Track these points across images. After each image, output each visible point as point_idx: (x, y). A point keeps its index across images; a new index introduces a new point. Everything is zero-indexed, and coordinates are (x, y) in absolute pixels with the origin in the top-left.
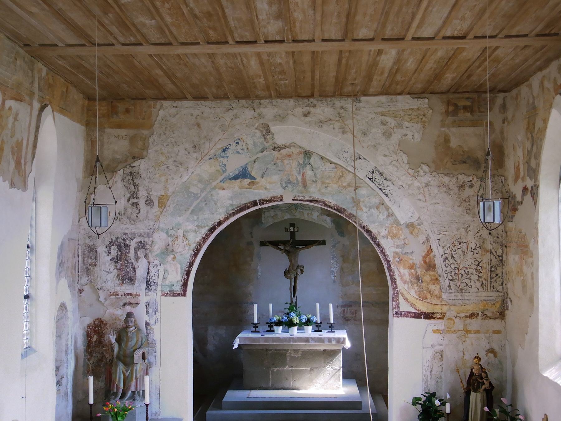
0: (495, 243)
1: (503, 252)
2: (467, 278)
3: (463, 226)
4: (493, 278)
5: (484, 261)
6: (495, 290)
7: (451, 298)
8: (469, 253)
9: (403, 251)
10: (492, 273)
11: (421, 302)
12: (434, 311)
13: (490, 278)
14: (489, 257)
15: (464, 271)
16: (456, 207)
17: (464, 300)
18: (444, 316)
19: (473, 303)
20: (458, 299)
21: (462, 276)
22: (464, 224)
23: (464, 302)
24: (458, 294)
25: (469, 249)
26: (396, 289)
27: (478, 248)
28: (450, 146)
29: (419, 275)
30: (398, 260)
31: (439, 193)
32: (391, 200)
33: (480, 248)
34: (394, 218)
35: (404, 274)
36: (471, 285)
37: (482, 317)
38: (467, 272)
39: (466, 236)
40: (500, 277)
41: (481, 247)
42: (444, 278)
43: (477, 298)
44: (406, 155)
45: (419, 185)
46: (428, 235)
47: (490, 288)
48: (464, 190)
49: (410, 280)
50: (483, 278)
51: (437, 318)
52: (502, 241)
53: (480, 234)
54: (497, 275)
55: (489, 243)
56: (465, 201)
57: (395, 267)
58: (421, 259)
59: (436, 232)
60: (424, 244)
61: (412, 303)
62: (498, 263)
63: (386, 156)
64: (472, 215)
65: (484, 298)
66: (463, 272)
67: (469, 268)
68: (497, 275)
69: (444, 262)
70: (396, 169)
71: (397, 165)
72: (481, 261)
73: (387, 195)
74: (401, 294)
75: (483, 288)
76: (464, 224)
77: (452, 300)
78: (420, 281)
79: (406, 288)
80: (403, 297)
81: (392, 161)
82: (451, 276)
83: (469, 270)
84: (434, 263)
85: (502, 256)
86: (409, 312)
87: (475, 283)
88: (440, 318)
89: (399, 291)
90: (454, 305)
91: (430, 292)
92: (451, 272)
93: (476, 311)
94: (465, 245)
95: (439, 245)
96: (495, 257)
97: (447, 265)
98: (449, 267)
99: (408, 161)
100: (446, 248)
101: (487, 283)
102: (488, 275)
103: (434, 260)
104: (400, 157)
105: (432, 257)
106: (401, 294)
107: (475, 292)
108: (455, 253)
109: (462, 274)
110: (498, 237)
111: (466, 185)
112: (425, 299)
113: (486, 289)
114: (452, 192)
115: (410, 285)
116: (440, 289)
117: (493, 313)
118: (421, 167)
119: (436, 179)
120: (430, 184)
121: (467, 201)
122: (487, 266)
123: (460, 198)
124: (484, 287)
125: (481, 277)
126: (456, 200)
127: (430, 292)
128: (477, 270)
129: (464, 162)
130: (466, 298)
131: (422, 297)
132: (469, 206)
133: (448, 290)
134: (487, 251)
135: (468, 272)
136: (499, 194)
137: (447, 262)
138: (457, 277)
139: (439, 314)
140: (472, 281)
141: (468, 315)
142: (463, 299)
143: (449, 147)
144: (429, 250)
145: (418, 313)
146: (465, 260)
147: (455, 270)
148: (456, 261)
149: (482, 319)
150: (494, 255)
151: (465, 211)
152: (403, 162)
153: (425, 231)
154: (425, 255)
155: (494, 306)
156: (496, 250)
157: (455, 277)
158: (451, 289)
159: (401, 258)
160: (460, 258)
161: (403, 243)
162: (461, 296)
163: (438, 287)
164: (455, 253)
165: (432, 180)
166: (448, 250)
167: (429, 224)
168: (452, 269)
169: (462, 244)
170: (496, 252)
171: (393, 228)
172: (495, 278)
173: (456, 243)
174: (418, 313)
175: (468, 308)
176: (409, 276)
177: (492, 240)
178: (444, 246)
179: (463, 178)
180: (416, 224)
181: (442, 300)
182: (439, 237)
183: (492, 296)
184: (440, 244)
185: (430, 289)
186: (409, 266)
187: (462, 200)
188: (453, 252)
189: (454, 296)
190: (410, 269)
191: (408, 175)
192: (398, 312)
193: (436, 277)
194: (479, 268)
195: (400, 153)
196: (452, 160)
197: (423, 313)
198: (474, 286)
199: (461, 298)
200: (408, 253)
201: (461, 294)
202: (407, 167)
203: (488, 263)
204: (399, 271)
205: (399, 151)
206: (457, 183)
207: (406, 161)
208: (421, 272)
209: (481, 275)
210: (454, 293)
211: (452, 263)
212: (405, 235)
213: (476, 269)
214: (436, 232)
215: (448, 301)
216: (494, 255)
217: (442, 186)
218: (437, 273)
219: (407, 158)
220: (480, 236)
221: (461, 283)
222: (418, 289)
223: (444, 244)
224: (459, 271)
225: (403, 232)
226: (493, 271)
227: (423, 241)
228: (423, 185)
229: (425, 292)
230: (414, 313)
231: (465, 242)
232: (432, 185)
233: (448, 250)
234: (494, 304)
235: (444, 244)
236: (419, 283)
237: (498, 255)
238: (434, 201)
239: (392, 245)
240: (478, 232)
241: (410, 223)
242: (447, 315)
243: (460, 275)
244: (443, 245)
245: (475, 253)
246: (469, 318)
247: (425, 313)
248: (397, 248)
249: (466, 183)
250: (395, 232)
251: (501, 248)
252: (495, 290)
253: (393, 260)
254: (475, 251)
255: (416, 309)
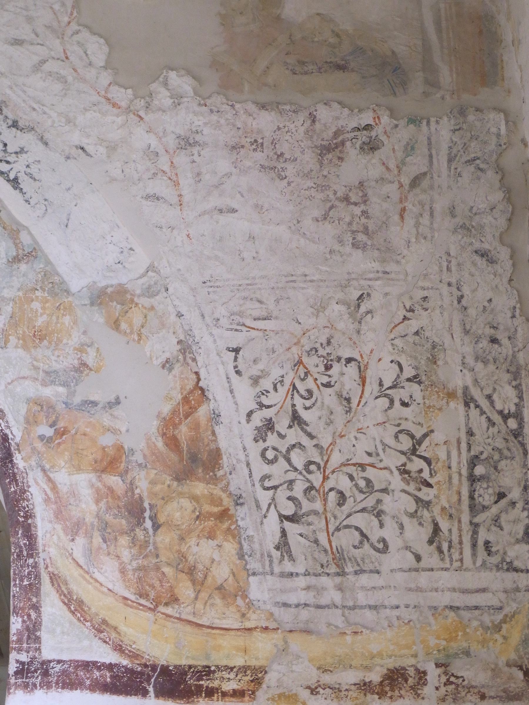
0: (485, 362)
1: (521, 398)
2: (363, 510)
3: (340, 295)
4: (485, 508)
5: (438, 437)
6: (495, 560)
7: (293, 599)
8: (372, 403)
9: (72, 394)
10: (477, 485)
11: (149, 615)
12: (207, 657)
13: (472, 507)
14: (462, 420)
15: (351, 478)
16: (308, 223)
17: (353, 608)
18: (257, 682)
19: (396, 623)
20: (323, 601)
21: (342, 498)
22: (344, 287)
23: (355, 616)
24: (324, 579)
25: (372, 388)
26: (30, 556)
27: (409, 380)
28: (283, 17)
29: (141, 498)
30: (49, 432)
31: (234, 170)
32: (32, 202)
33: (420, 383)
34: (39, 266)
35: (73, 494)
36: (383, 541)
37: (443, 690)
38: (362, 484)
39: (355, 337)
40: (513, 504)
41: (424, 378)
42: (258, 506)
43: (412, 598)
44: (102, 41)
45: (154, 143)
46: (189, 333)
47: (474, 555)
48: (341, 159)
49: (97, 516)
50: (436, 510)
51: (224, 694)
52: (514, 356)
53: (414, 325)
54: (501, 496)
55: (458, 360)
56: (346, 199)
57: (33, 463)
58: (154, 430)
59: (224, 322)
60: (170, 370)
61: (104, 622)
62: (499, 443)
63: (18, 42)
64: (376, 254)
65: (446, 599)
66: (345, 484)
67: (372, 465)
68: (501, 496)
69: (256, 440)
70: (58, 87)
71: (63, 72)
72: (425, 436)
73: (15, 183)
74: (54, 578)
75: (440, 550)
76: (344, 287)
77: (297, 606)
78: (148, 524)
79: (78, 555)
80: (61, 593)
81: (44, 62)
82: (289, 498)
83: (370, 473)
84: (213, 446)
85: (518, 416)
86: (87, 665)
87: (402, 527)
88: (239, 694)
89: (42, 566)
90: (307, 632)
91: (191, 571)
92: (291, 483)
93: (412, 661)
94: (352, 370)
95: (238, 373)
96: (489, 419)
97: (270, 454)
98: (281, 460)
99: (107, 62)
100: (266, 384)
101: (455, 531)
102: (459, 493)
103: (214, 433)
104: (76, 48)
105: (203, 421)
106: (54, 578)
107: (401, 570)
108: (308, 403)
109: (341, 494)
110: (494, 341)
111: (348, 144)
112: (166, 604)
113: (456, 556)
114: (291, 170)
115: (97, 540)
116: (241, 556)
117: (495, 671)
118: (161, 79)
119: (222, 121)
120: (198, 138)
121: (353, 199)
122: (454, 453)
123: (322, 188)
124: (445, 546)
125: (427, 504)
126: (311, 198)
127: (191, 571)
128: (408, 472)
129: (341, 68)
130: (362, 598)
131: (152, 595)
132: (363, 220)
133: (276, 561)
134: (451, 395)
135: (368, 482)
136: (490, 174)
137: (272, 439)
138: (318, 505)
139: (232, 675)
140: (387, 520)
141: (375, 677)
142: (351, 604)
143: (278, 18)
144: (191, 392)
145: (131, 671)
146: (354, 433)
147: (310, 472)
148: (311, 436)
149: (443, 700)
150: (483, 413)
151: (348, 238)
152: (90, 64)
153: (173, 318)
154: (174, 412)
155: (497, 636)
156: (488, 391)
157: (306, 506)
158: (292, 559)
159: (61, 424)
160: (331, 422)
161: (76, 362)
162: (340, 588)
163: (230, 547)
164: (308, 403)
165: (205, 124)
166: (275, 389)
167: (193, 290)
168: (296, 469)
169: (336, 368)
170: (489, 397)
171: (36, 305)
172: (494, 510)
173: (311, 362)
174: (128, 670)
175: (375, 648)
176: (97, 502)
177: (468, 349)
178: (259, 377)
179: (338, 118)
180: (138, 292)
181: (250, 605)
182: (237, 340)
183: (484, 590)
184: (240, 368)
185: (191, 559)
186: (99, 457)
187: (332, 196)
188: (298, 401)
189: (308, 588)
190: (103, 471)
191: (109, 107)
192: (30, 663)
193: (221, 504)
194: (416, 464)
195: (77, 32)
196: (291, 60)
197: (154, 668)
198: (400, 543)
199: (337, 597)
200: (94, 404)
201: (338, 580)
202: (105, 78)
203: (459, 442)
204: (49, 480)
205: (74, 27)
206: (312, 137)
207: (99, 59)
208: (153, 483)
209: (426, 494)
210: (307, 574)
211: (294, 446)
212: (85, 333)
213: (404, 471)
214: (224, 322)
215: (276, 611)
216: (483, 413)
217: (247, 145)
218: (225, 489)
219: (106, 49)
220: (417, 333)
221: (338, 529)
222: (134, 558)
223: (261, 366)
224: (325, 478)
225: (75, 322)
226: (482, 478)
227: (167, 355)
228: (171, 142)
229: (166, 570)
230: (110, 667)
231: (349, 360)
232: (206, 144)
233: (275, 389)
234: (498, 628)
235: (261, 366)
236: (140, 534)
237: (501, 413)
238: (215, 201)
239: (26, 372)
240: (405, 318)
241: (112, 286)
242: (271, 678)
243: (332, 496)
244: (255, 371)
245: (397, 403)
246: (381, 694)
247: (165, 670)
248: (44, 384)
249: (352, 135)
250: (40, 321)
251: (510, 384)
252: (495, 560)
253: (27, 432)
254: (397, 394)
255: (119, 649)
